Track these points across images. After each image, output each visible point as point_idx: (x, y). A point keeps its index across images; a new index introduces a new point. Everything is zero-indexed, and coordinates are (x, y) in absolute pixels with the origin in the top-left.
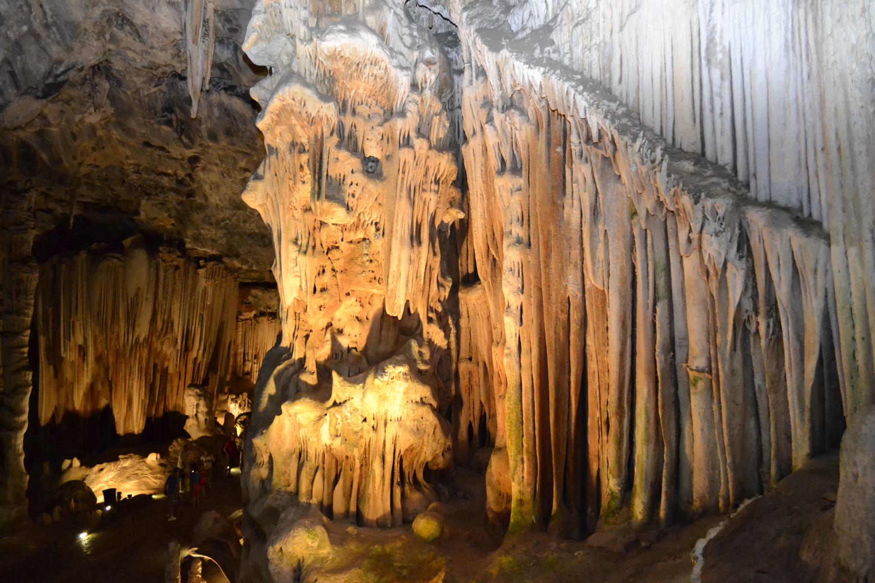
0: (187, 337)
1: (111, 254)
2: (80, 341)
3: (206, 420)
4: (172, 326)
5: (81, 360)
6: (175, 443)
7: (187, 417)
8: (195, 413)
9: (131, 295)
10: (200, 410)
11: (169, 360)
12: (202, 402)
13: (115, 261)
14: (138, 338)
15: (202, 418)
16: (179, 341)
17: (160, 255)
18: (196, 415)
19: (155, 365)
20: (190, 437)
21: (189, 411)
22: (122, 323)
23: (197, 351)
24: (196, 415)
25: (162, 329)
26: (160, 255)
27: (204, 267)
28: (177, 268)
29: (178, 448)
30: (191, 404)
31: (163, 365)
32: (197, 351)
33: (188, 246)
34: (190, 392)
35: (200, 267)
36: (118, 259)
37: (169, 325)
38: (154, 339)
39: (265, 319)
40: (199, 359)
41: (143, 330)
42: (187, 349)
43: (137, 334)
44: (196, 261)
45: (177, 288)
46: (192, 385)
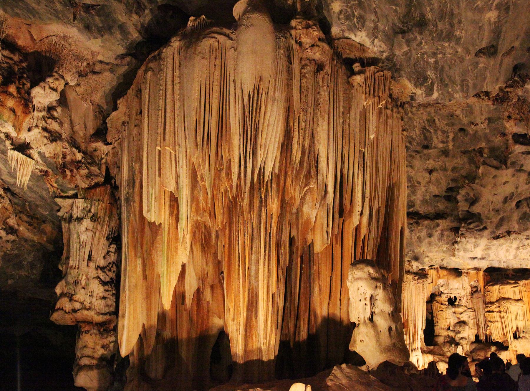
0: (342, 184)
1: (214, 29)
2: (171, 187)
3: (390, 329)
4: (317, 167)
5: (172, 221)
6: (336, 371)
7: (353, 326)
8: (368, 315)
9: (249, 87)
10: (377, 310)
11: (313, 229)
12: (380, 294)
13: (221, 38)
14: (262, 171)
15: (383, 323)
16: (331, 189)
17: (293, 32)
18: (371, 319)
19: (292, 241)
20: (362, 362)
21: (358, 312)
22: (236, 141)
23: (359, 218)
24: (371, 319)
25: (301, 163)
26: (293, 32)
27: (360, 73)
28: (320, 67)
29: (344, 381)
30: (360, 296)
31: (305, 242)
32: (359, 218)
33: (335, 30)
34: (358, 273)
35: (353, 73)
36: (228, 36)
37: (311, 164)
38: (289, 181)
39: (411, 277)
40: (364, 231)
41: (269, 157)
42: (342, 211)
43: (259, 160)
44: (349, 63)
45: (321, 101)
46: (357, 262)
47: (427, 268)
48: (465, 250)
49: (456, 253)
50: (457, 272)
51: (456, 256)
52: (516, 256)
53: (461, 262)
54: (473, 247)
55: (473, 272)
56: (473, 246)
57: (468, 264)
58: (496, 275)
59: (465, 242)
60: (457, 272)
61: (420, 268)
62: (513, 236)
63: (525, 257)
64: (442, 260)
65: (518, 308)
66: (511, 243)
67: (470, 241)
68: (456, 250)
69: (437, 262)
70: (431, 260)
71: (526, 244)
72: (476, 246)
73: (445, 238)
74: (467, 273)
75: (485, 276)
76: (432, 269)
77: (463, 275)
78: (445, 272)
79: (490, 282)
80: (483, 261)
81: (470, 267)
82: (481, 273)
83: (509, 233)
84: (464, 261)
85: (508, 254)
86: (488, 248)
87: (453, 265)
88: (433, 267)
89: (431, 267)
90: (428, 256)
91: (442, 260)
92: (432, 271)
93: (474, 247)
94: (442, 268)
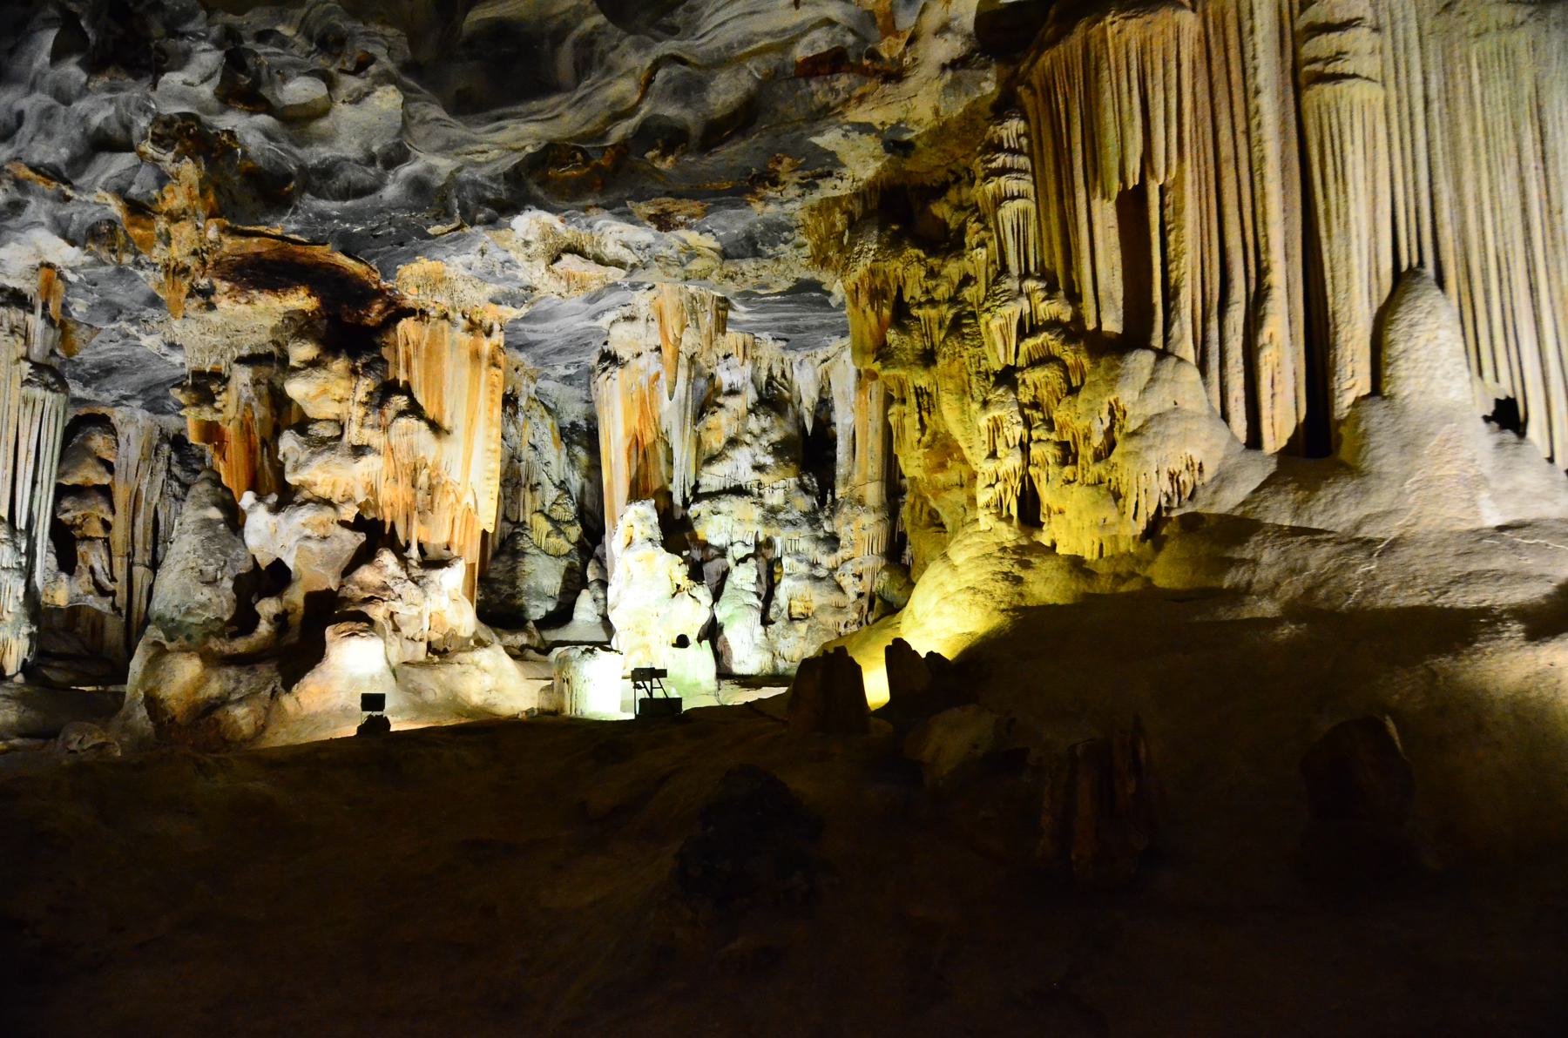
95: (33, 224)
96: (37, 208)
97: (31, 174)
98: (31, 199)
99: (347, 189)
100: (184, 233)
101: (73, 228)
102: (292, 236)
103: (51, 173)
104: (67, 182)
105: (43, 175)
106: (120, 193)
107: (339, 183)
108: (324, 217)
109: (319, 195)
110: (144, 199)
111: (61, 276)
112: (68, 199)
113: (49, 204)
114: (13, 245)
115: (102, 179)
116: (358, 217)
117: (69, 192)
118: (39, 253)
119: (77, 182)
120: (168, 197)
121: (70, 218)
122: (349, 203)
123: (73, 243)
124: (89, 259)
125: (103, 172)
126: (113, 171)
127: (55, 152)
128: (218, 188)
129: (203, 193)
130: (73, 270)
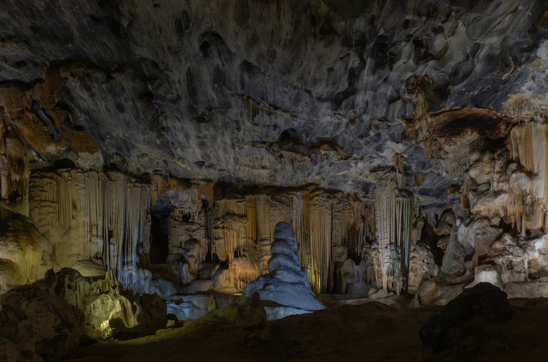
47: (150, 171)
48: (183, 148)
49: (173, 150)
50: (187, 183)
51: (177, 157)
52: (237, 161)
53: (189, 169)
54: (185, 141)
55: (202, 183)
56: (183, 136)
57: (198, 174)
58: (225, 188)
59: (173, 129)
60: (187, 183)
61: (143, 170)
62: (219, 119)
63: (246, 163)
64: (165, 162)
65: (241, 224)
66: (223, 135)
67: (177, 128)
68: (171, 145)
69: (160, 164)
70: (151, 160)
71: (241, 139)
72: (187, 136)
73: (142, 116)
74: (197, 184)
75: (215, 189)
76: (157, 174)
77: (193, 186)
78: (174, 182)
79: (218, 197)
80: (212, 170)
81: (201, 177)
82: (212, 185)
83: (210, 109)
84: (192, 169)
85: (228, 156)
86: (202, 145)
87: (182, 175)
88: (159, 172)
89: (156, 172)
90: (146, 155)
91: (165, 162)
92: (157, 176)
93: (187, 140)
94: (172, 176)
95: (386, 140)
96: (384, 134)
97: (379, 122)
98: (380, 131)
99: (464, 76)
100: (424, 123)
101: (396, 137)
102: (454, 108)
103: (385, 119)
104: (388, 121)
105: (382, 121)
106: (403, 117)
107: (460, 75)
108: (461, 93)
109: (454, 84)
110: (411, 117)
111: (402, 157)
112: (390, 126)
113: (386, 131)
114: (386, 150)
115: (396, 115)
116: (471, 87)
117: (390, 124)
118: (393, 150)
119: (389, 119)
120: (417, 112)
121: (394, 134)
122: (465, 82)
123: (397, 143)
124: (406, 147)
125: (394, 111)
126: (397, 110)
127: (381, 112)
128: (428, 100)
129: (425, 106)
130: (404, 152)
